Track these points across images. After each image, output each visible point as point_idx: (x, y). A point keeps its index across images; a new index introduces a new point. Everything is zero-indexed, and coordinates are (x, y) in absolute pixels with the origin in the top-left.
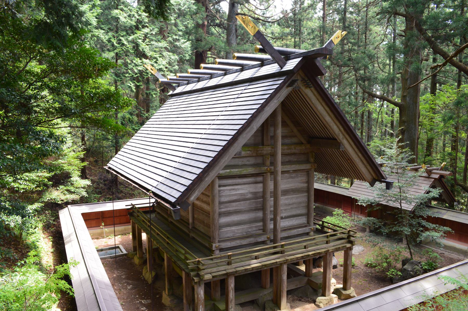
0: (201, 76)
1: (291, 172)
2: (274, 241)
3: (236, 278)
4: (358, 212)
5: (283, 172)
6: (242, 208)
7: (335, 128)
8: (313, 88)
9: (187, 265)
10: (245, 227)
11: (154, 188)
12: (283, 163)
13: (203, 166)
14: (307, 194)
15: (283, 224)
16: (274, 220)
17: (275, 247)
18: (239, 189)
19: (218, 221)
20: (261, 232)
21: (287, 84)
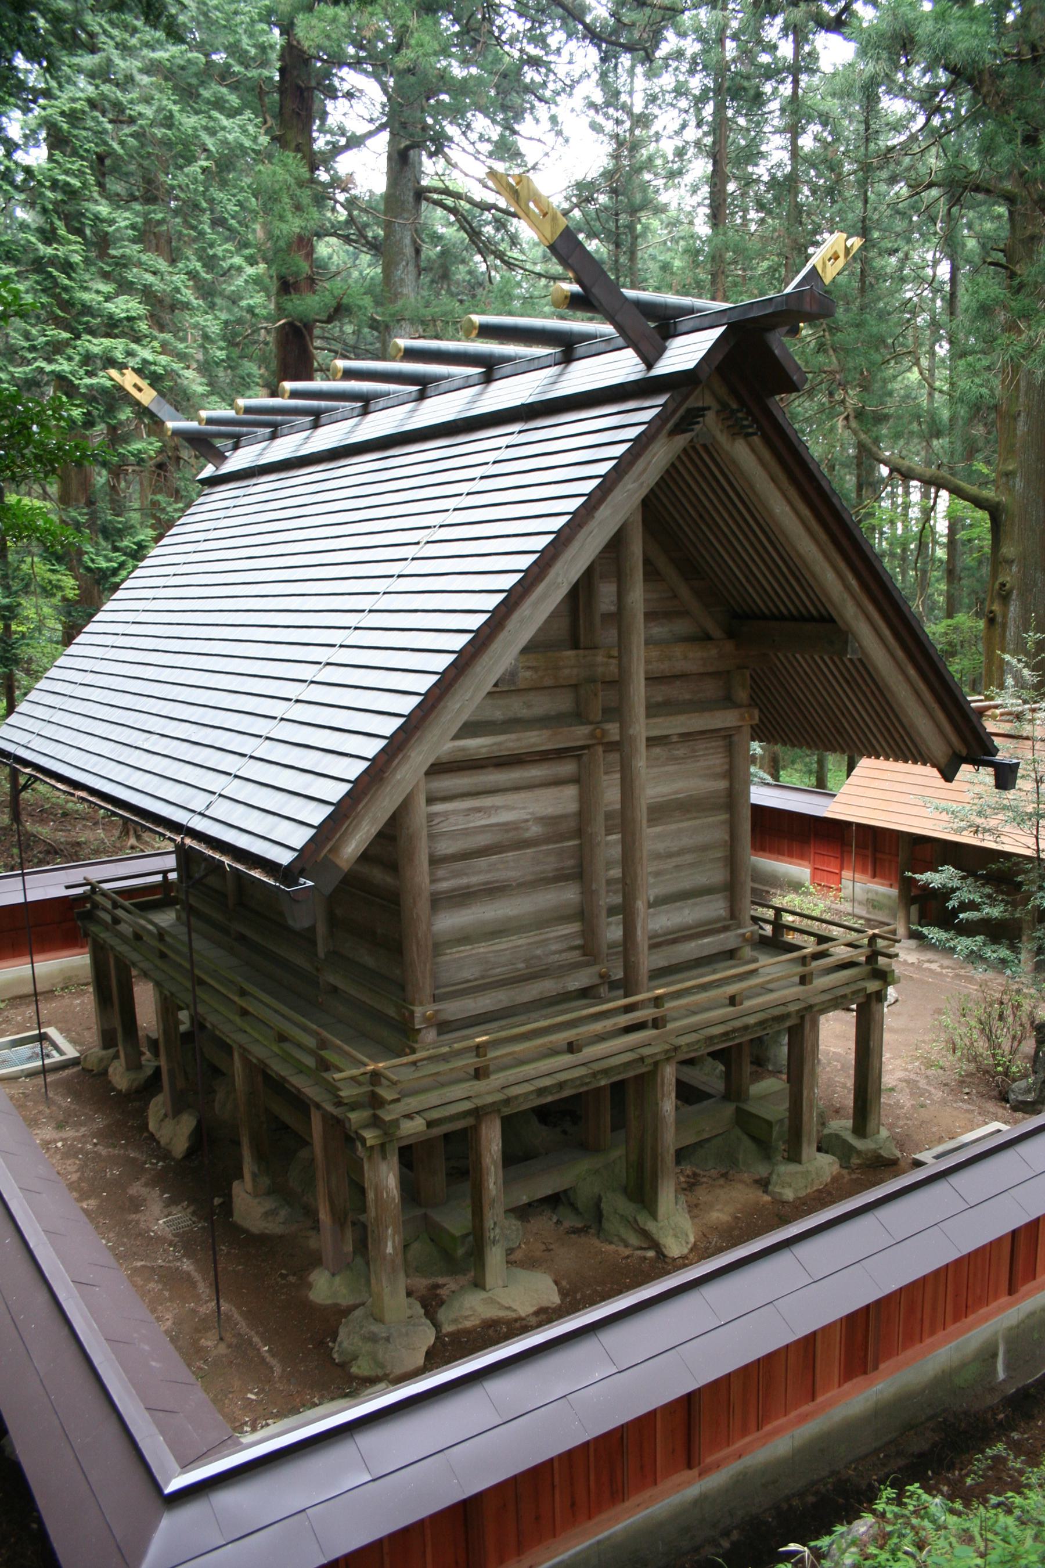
0: (323, 404)
1: (675, 739)
2: (627, 985)
3: (508, 1123)
4: (864, 871)
5: (651, 742)
6: (512, 874)
7: (833, 582)
8: (756, 440)
9: (332, 1089)
10: (520, 941)
11: (198, 818)
12: (653, 709)
13: (389, 726)
14: (725, 817)
15: (663, 921)
16: (626, 911)
17: (629, 1009)
18: (497, 808)
19: (430, 924)
20: (575, 956)
21: (670, 425)
